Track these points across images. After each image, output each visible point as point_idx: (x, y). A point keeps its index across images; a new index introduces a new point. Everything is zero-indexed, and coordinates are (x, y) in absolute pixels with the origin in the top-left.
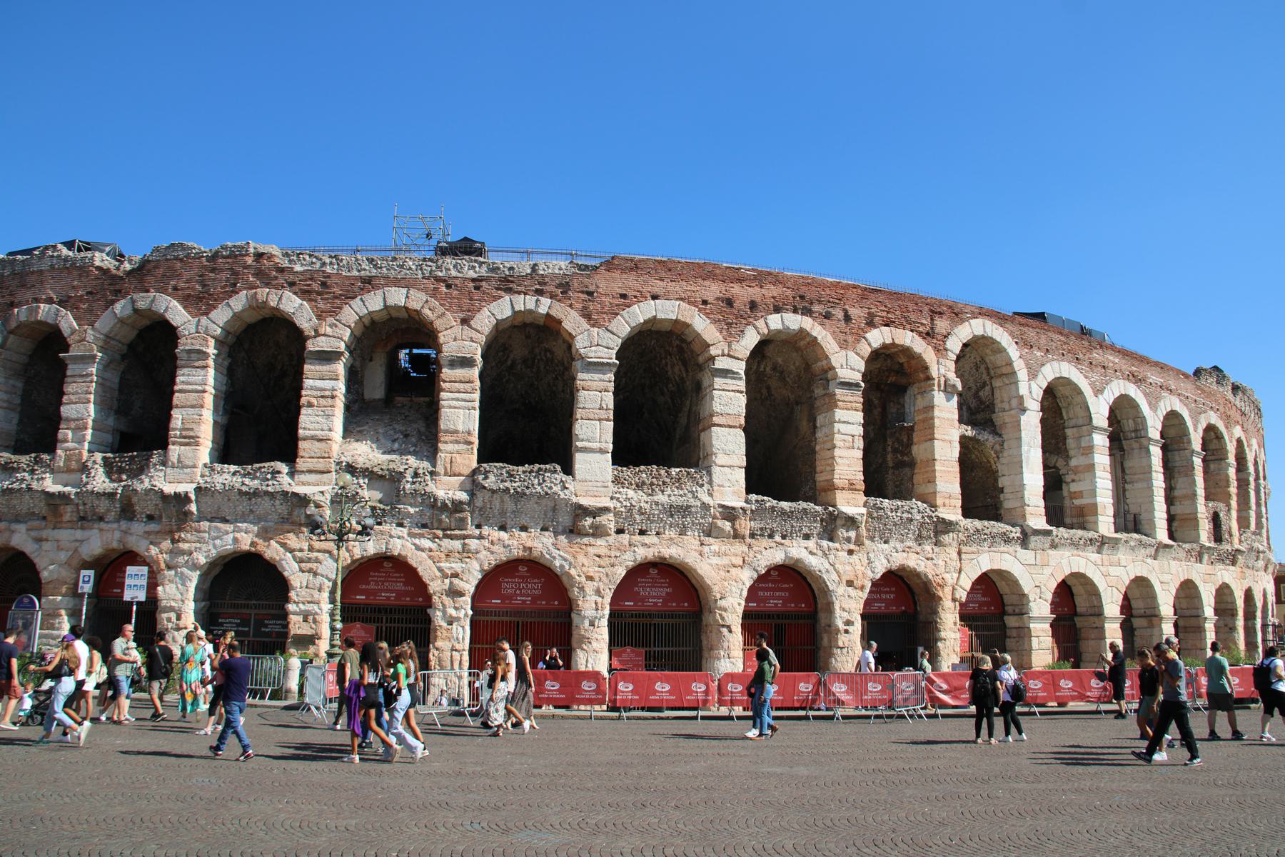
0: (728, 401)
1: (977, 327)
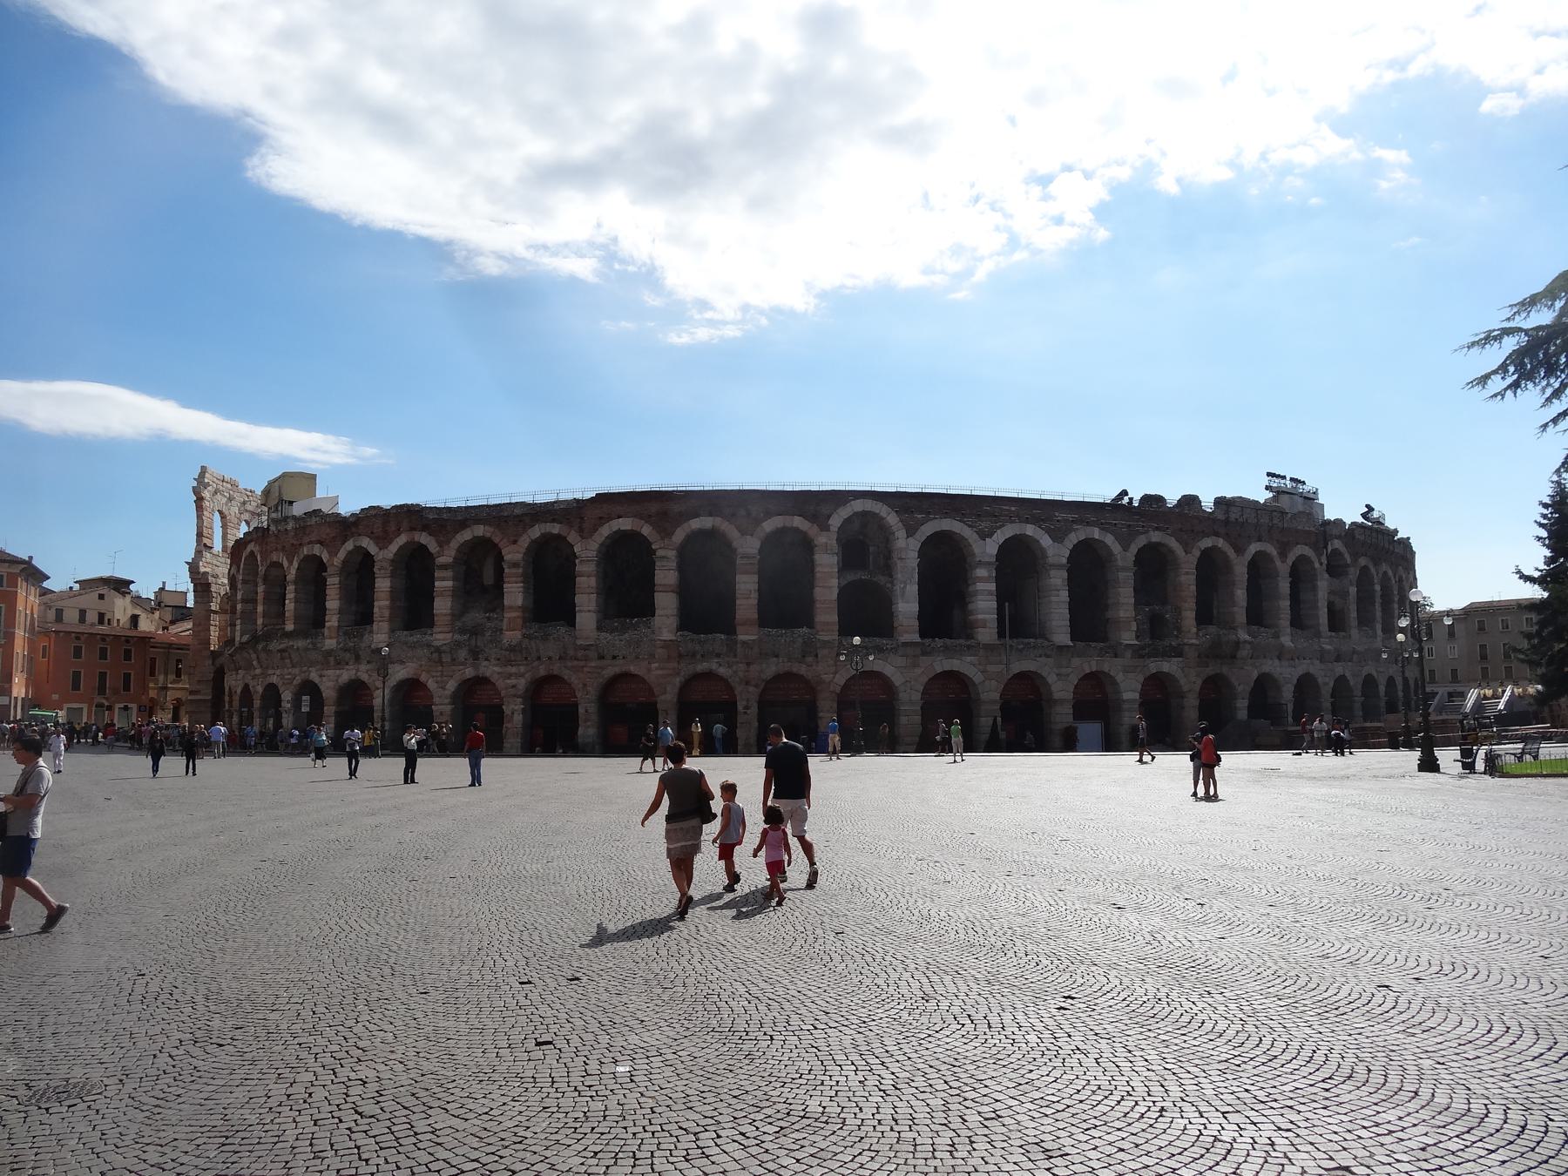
0: (666, 575)
1: (858, 506)
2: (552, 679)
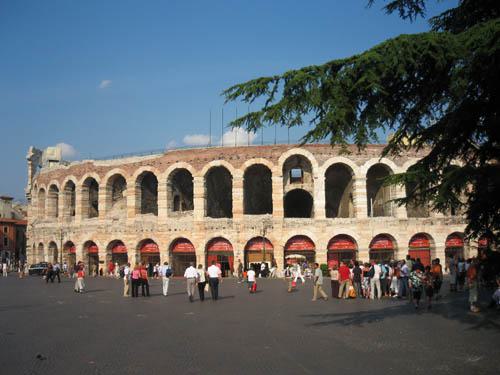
0: (199, 188)
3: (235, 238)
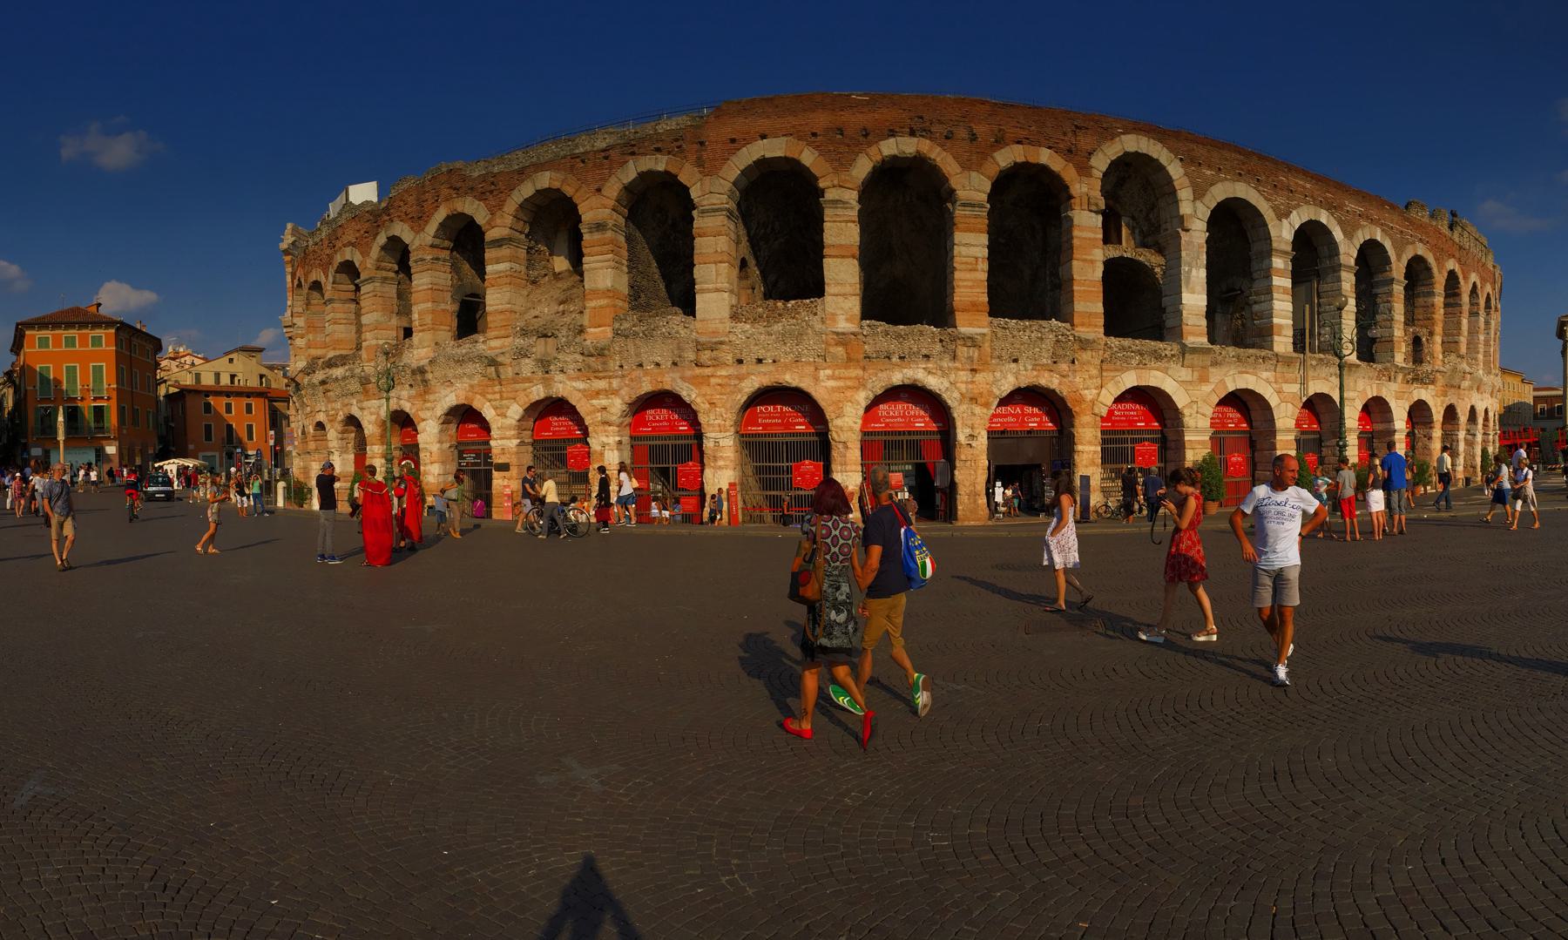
0: (842, 231)
2: (664, 399)
3: (963, 387)
